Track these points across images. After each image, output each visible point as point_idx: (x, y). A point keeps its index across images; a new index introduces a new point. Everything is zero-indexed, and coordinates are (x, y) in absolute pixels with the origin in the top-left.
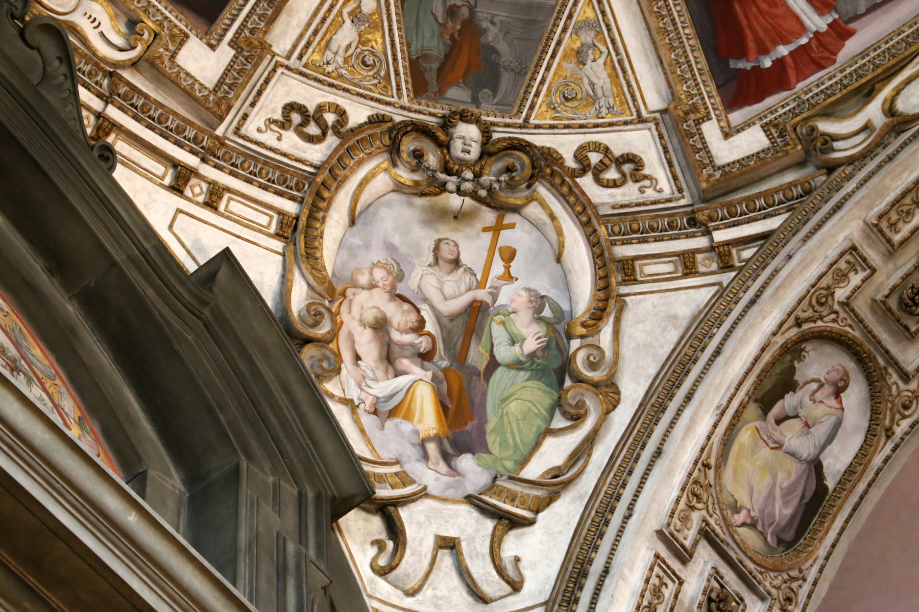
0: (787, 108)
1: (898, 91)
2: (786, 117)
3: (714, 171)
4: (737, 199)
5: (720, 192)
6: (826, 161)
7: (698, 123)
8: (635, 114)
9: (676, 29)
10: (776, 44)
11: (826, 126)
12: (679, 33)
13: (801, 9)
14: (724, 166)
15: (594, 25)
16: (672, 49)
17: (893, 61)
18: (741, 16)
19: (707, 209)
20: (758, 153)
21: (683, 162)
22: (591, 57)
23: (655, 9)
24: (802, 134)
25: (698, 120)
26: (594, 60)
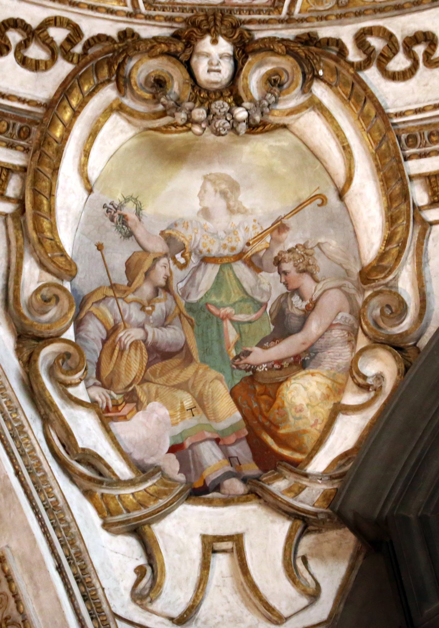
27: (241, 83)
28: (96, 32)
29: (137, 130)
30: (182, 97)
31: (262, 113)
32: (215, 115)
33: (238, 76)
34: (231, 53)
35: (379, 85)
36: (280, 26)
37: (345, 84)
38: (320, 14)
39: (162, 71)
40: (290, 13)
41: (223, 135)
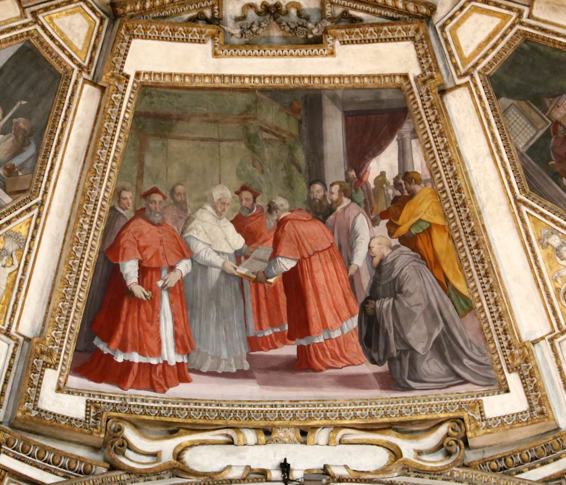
0: (112, 401)
1: (192, 445)
2: (107, 406)
3: (33, 409)
4: (35, 442)
5: (27, 427)
6: (113, 459)
7: (46, 365)
8: (6, 326)
9: (75, 287)
10: (134, 349)
11: (129, 434)
12: (75, 292)
13: (166, 338)
14: (42, 411)
15: (21, 241)
16: (64, 299)
17: (202, 421)
18: (124, 313)
19: (9, 433)
20: (72, 419)
21: (16, 387)
22: (4, 262)
23: (70, 262)
24: (110, 428)
25: (47, 364)
26: (4, 266)
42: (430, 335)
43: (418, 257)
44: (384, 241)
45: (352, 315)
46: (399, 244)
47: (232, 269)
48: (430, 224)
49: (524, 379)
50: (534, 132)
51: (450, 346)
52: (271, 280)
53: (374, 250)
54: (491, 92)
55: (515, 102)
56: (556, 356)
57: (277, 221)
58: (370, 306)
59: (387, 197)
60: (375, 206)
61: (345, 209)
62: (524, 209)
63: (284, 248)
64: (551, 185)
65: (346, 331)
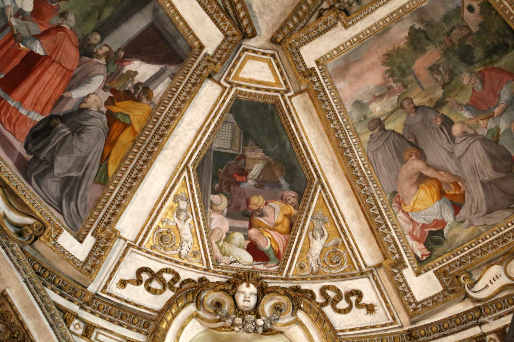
27: (260, 308)
28: (187, 277)
29: (205, 329)
30: (230, 313)
31: (271, 323)
32: (247, 322)
33: (259, 304)
34: (256, 293)
35: (332, 315)
36: (281, 281)
37: (315, 312)
38: (302, 277)
39: (220, 299)
40: (287, 275)
41: (250, 333)
42: (70, 171)
43: (106, 130)
44: (99, 102)
45: (42, 113)
46: (105, 112)
47: (10, 15)
48: (131, 124)
49: (96, 246)
50: (229, 147)
51: (73, 188)
52: (22, 46)
53: (89, 99)
54: (231, 105)
55: (235, 124)
56: (124, 255)
57: (59, 24)
58: (56, 121)
59: (125, 85)
60: (114, 82)
61: (98, 63)
62: (185, 174)
63: (47, 40)
64: (209, 180)
65: (30, 116)
